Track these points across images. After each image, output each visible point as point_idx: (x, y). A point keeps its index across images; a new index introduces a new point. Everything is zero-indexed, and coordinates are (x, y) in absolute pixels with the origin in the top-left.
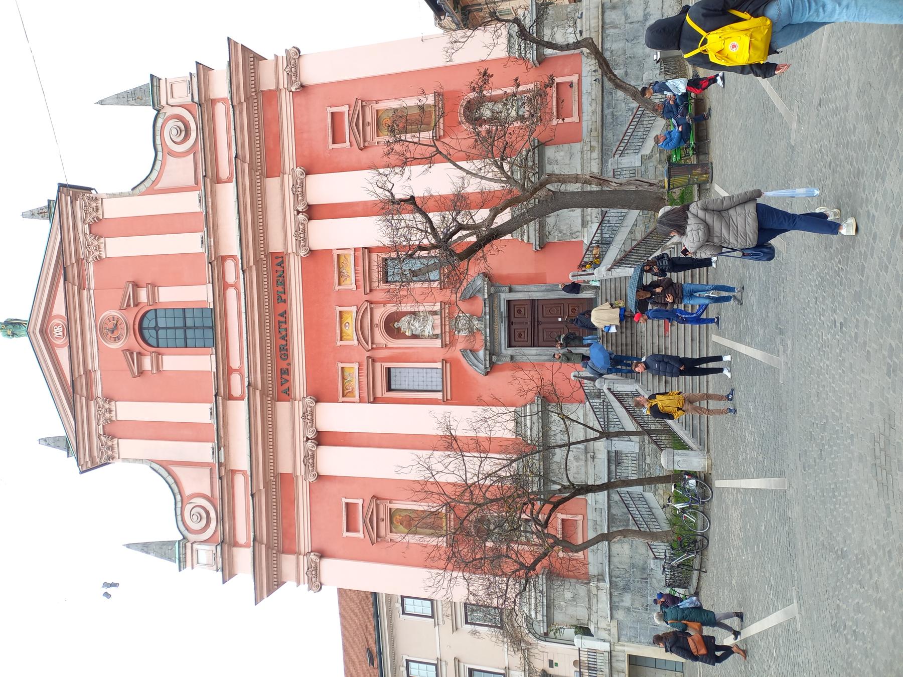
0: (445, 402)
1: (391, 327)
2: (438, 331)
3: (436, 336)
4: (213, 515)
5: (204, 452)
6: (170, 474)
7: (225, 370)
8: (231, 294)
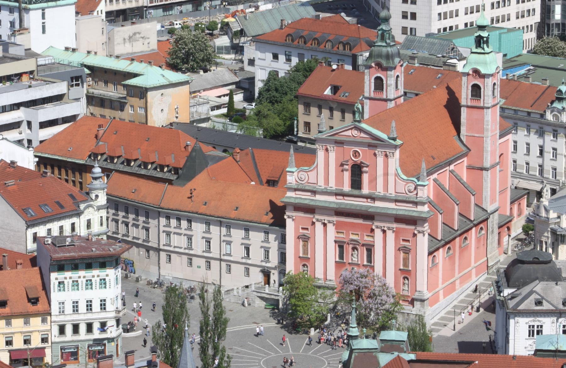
0: (336, 262)
1: (354, 249)
2: (353, 262)
3: (352, 260)
4: (303, 182)
5: (321, 184)
6: (314, 168)
7: (344, 195)
8: (365, 200)
